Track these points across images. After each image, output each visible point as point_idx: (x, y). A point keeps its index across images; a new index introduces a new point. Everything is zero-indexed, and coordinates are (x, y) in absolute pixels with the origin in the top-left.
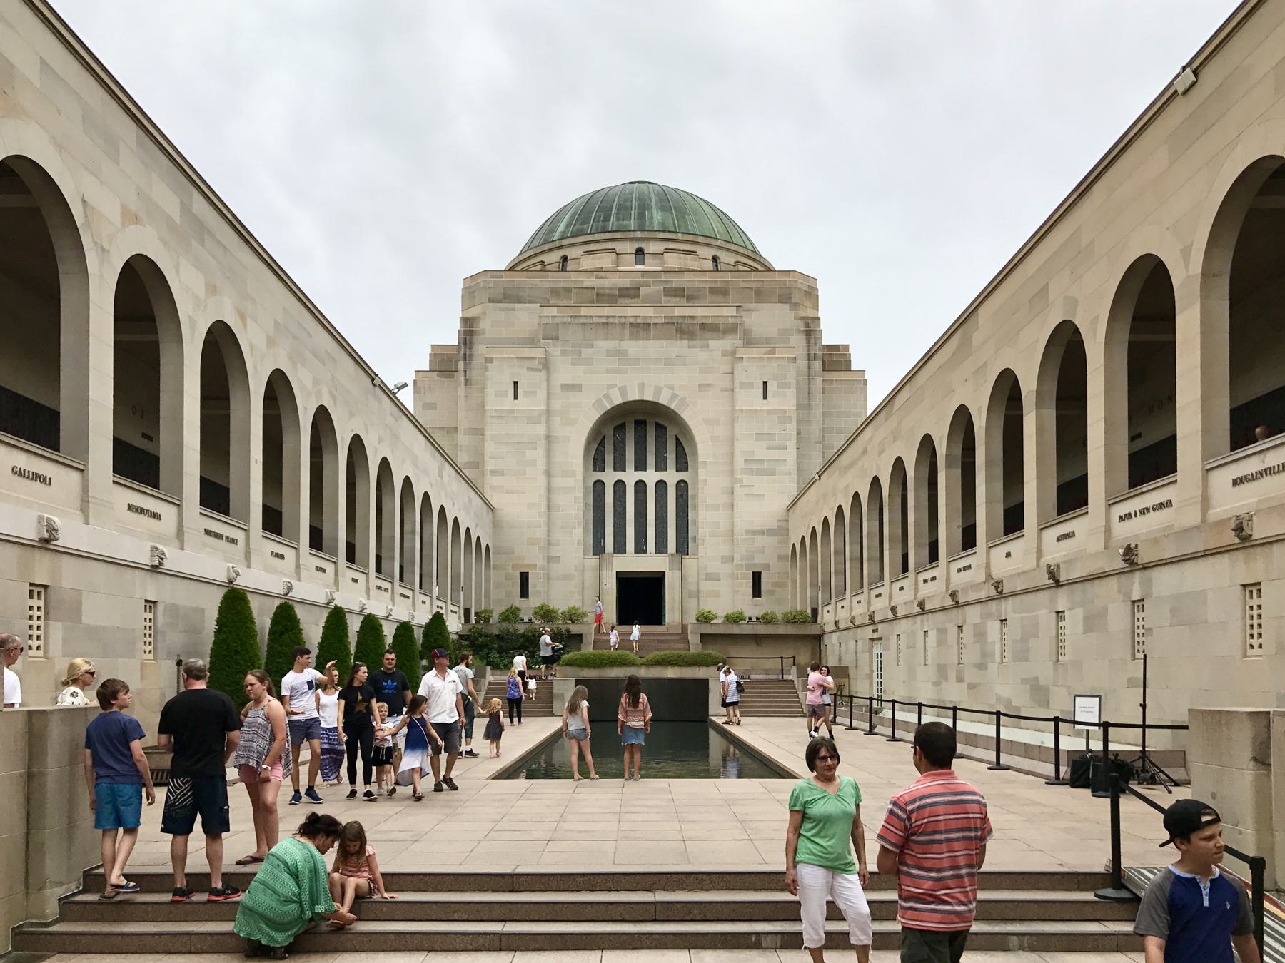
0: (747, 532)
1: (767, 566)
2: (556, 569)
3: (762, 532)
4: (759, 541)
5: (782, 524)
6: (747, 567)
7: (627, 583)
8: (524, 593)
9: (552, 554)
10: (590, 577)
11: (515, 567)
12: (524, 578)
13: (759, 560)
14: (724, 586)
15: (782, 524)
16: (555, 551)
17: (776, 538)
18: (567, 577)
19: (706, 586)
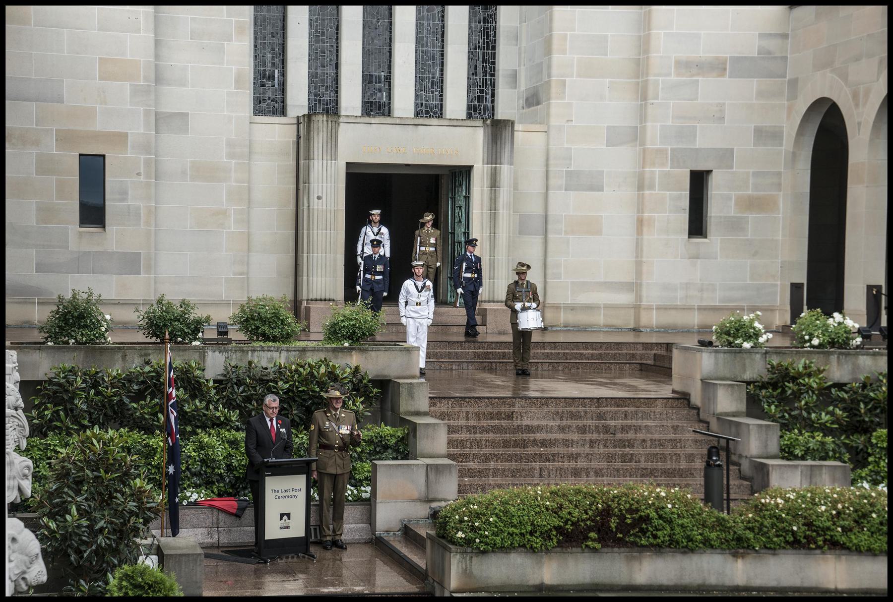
0: (687, 66)
1: (726, 156)
2: (177, 150)
3: (718, 67)
4: (712, 90)
5: (773, 45)
6: (677, 157)
7: (374, 191)
8: (93, 214)
9: (168, 107)
10: (270, 175)
11: (65, 138)
12: (92, 170)
13: (707, 140)
14: (613, 207)
15: (773, 45)
16: (174, 99)
17: (754, 84)
18: (206, 172)
19: (566, 204)
